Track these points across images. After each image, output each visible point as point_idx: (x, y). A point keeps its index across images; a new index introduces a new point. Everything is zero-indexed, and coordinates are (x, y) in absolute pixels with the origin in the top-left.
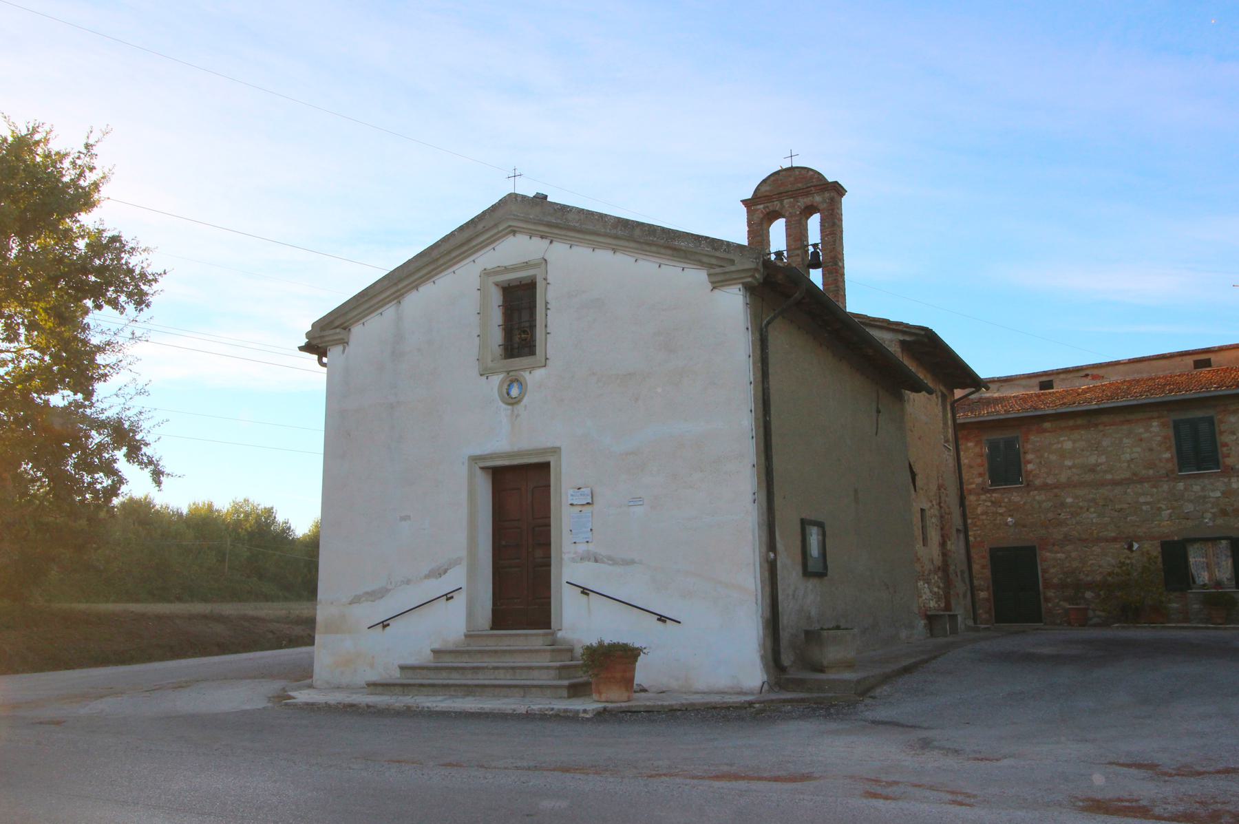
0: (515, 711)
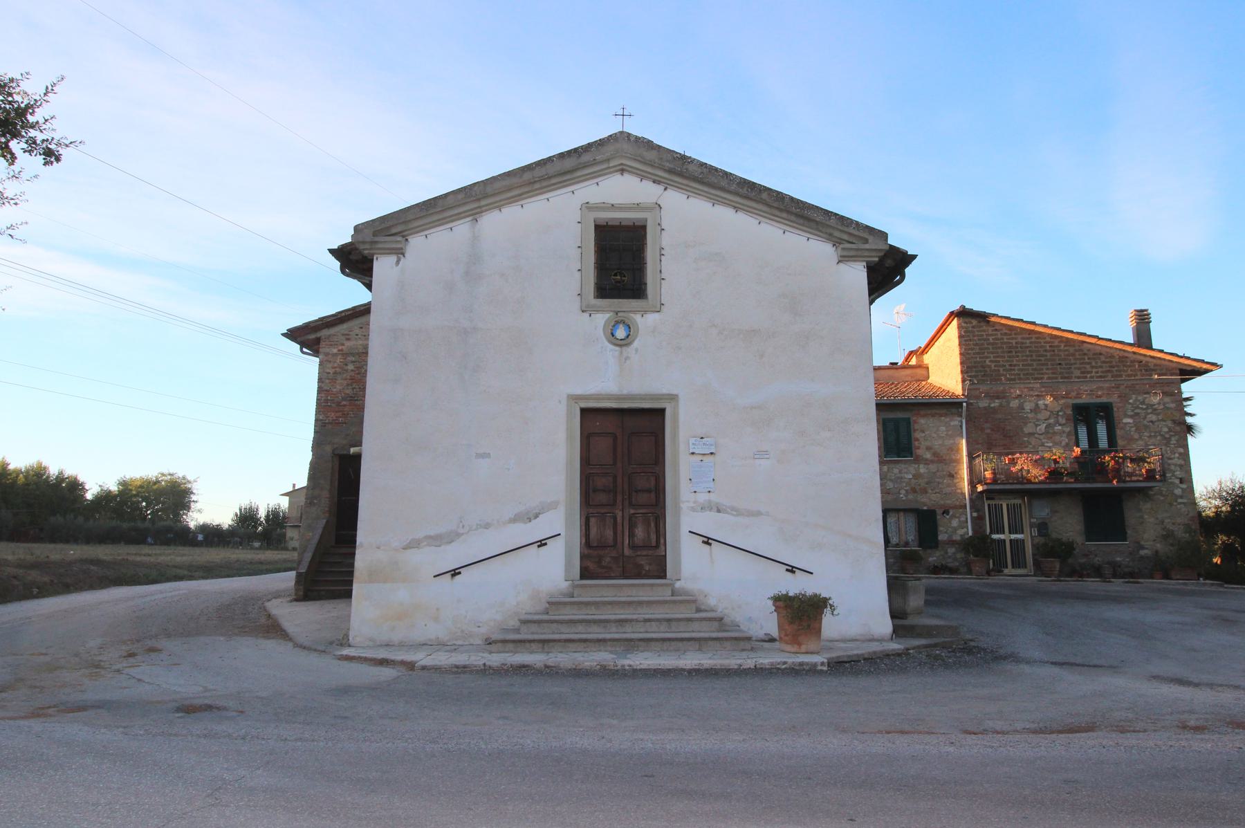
0: (741, 666)
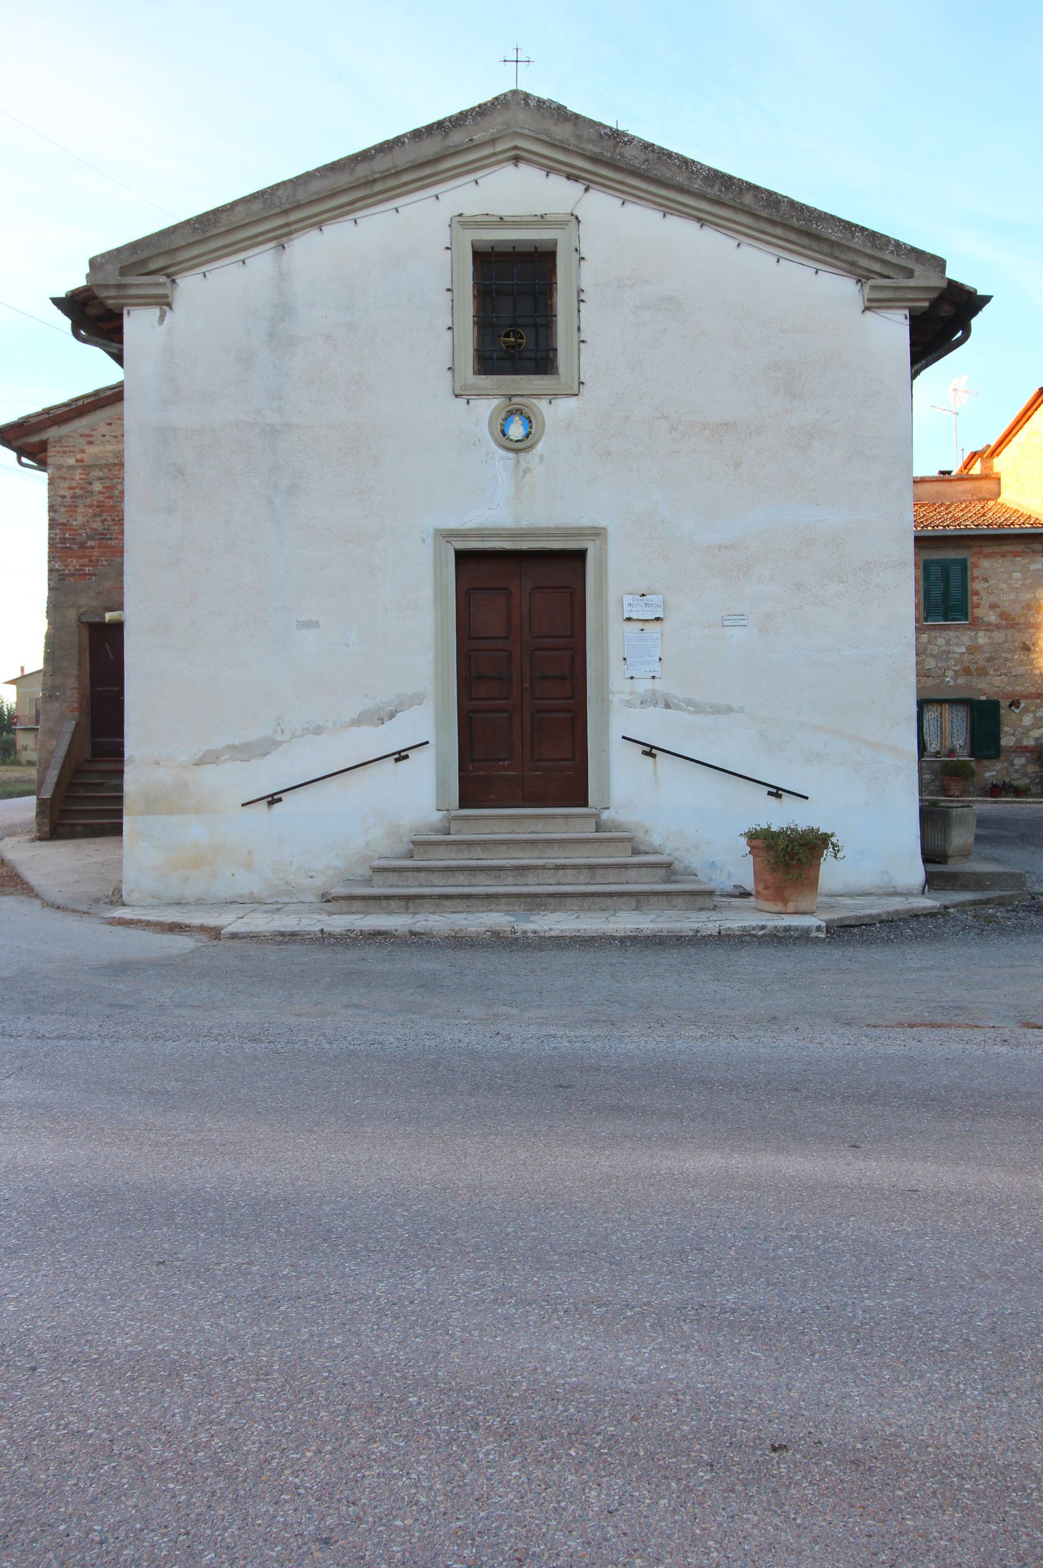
0: (698, 932)
